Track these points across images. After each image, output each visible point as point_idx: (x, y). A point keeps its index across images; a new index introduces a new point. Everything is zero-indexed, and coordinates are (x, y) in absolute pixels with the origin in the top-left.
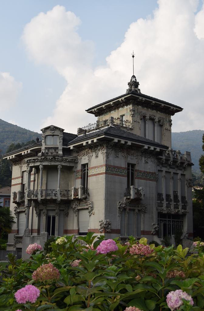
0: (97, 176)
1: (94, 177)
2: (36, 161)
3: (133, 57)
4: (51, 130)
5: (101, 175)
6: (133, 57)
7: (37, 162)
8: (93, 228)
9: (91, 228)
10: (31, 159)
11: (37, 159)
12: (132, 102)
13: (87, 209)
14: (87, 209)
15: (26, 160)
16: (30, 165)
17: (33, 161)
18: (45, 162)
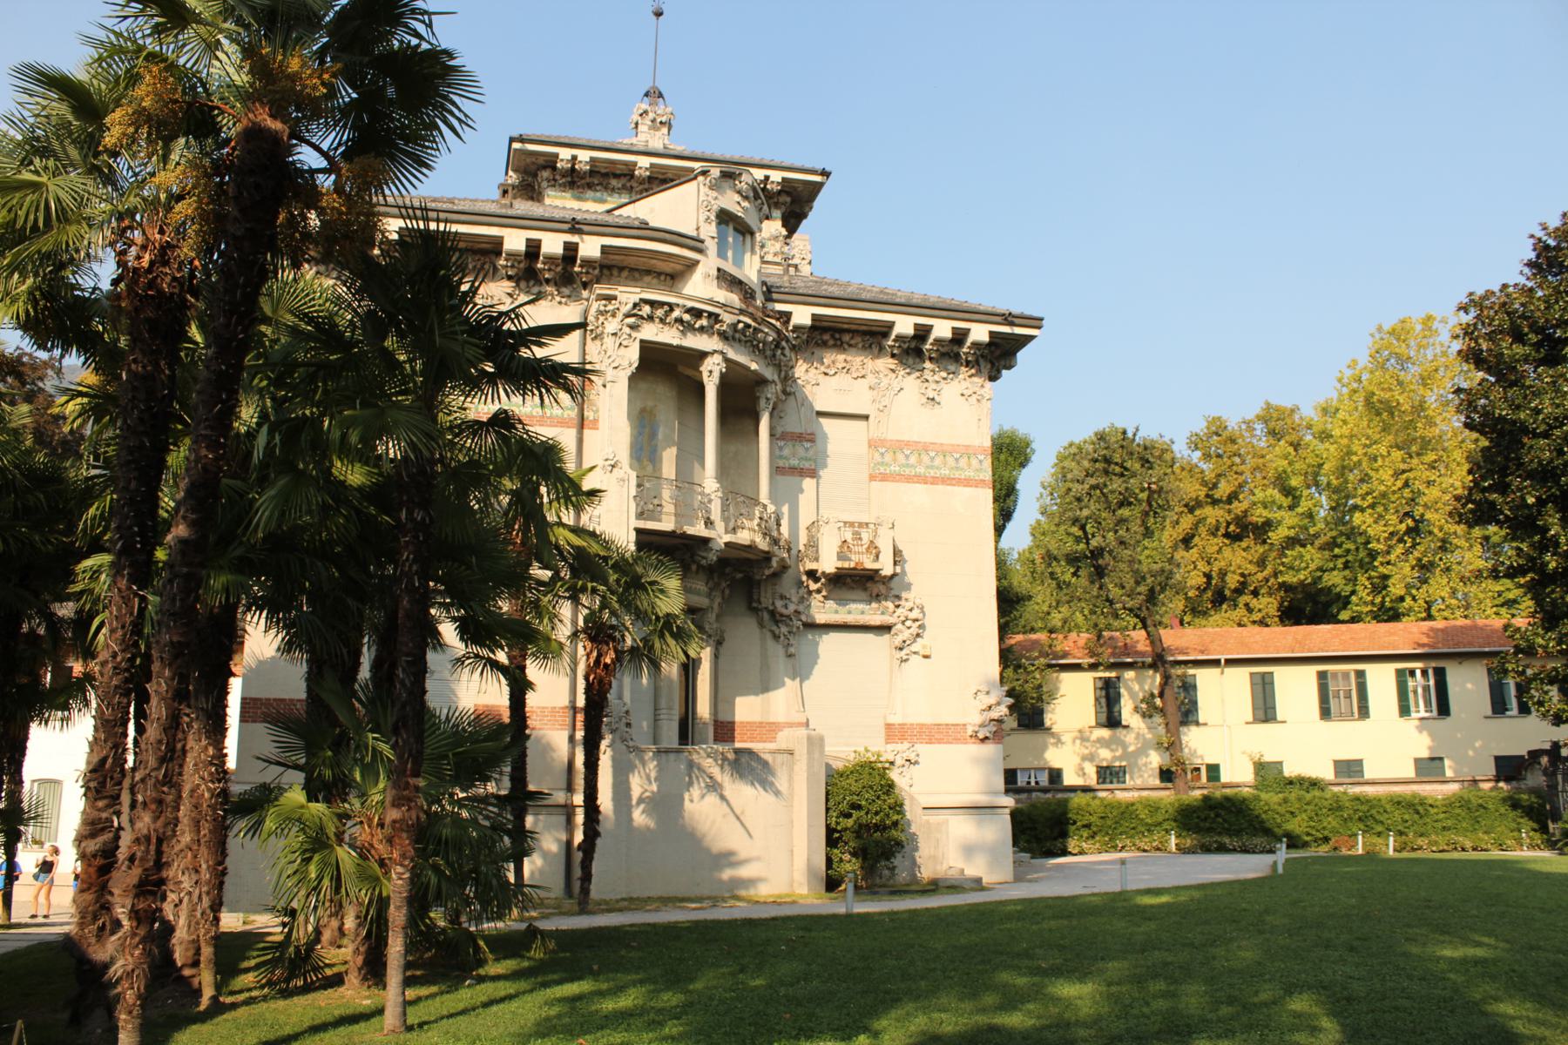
0: (940, 487)
1: (920, 488)
2: (704, 322)
3: (659, 14)
4: (739, 192)
5: (968, 490)
6: (659, 14)
7: (702, 329)
8: (928, 720)
9: (909, 720)
10: (671, 307)
11: (711, 314)
12: (784, 204)
13: (885, 629)
14: (885, 629)
15: (636, 298)
16: (651, 332)
17: (687, 317)
18: (736, 345)
